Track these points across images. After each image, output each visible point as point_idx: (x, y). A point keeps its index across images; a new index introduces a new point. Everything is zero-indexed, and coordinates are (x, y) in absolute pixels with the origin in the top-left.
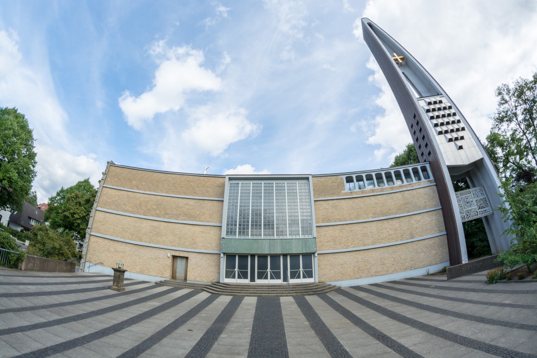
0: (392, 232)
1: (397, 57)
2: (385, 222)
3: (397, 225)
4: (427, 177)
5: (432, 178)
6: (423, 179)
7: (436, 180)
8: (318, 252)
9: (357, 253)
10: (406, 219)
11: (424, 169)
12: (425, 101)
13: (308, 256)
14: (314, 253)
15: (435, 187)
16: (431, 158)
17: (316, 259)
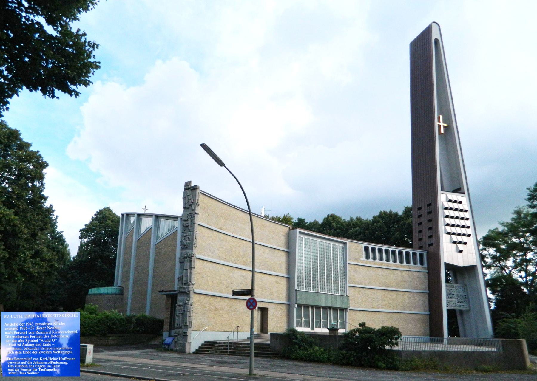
0: (390, 301)
1: (442, 124)
2: (387, 292)
3: (394, 297)
4: (422, 263)
5: (426, 265)
6: (419, 265)
7: (428, 268)
8: (351, 308)
9: (368, 312)
10: (402, 294)
11: (421, 255)
12: (447, 197)
13: (343, 310)
14: (346, 309)
15: (427, 274)
16: (431, 249)
17: (347, 313)
